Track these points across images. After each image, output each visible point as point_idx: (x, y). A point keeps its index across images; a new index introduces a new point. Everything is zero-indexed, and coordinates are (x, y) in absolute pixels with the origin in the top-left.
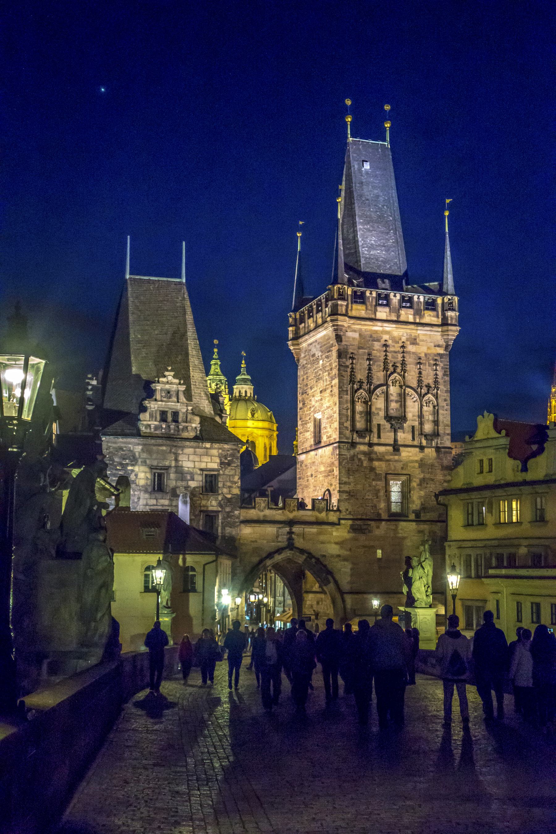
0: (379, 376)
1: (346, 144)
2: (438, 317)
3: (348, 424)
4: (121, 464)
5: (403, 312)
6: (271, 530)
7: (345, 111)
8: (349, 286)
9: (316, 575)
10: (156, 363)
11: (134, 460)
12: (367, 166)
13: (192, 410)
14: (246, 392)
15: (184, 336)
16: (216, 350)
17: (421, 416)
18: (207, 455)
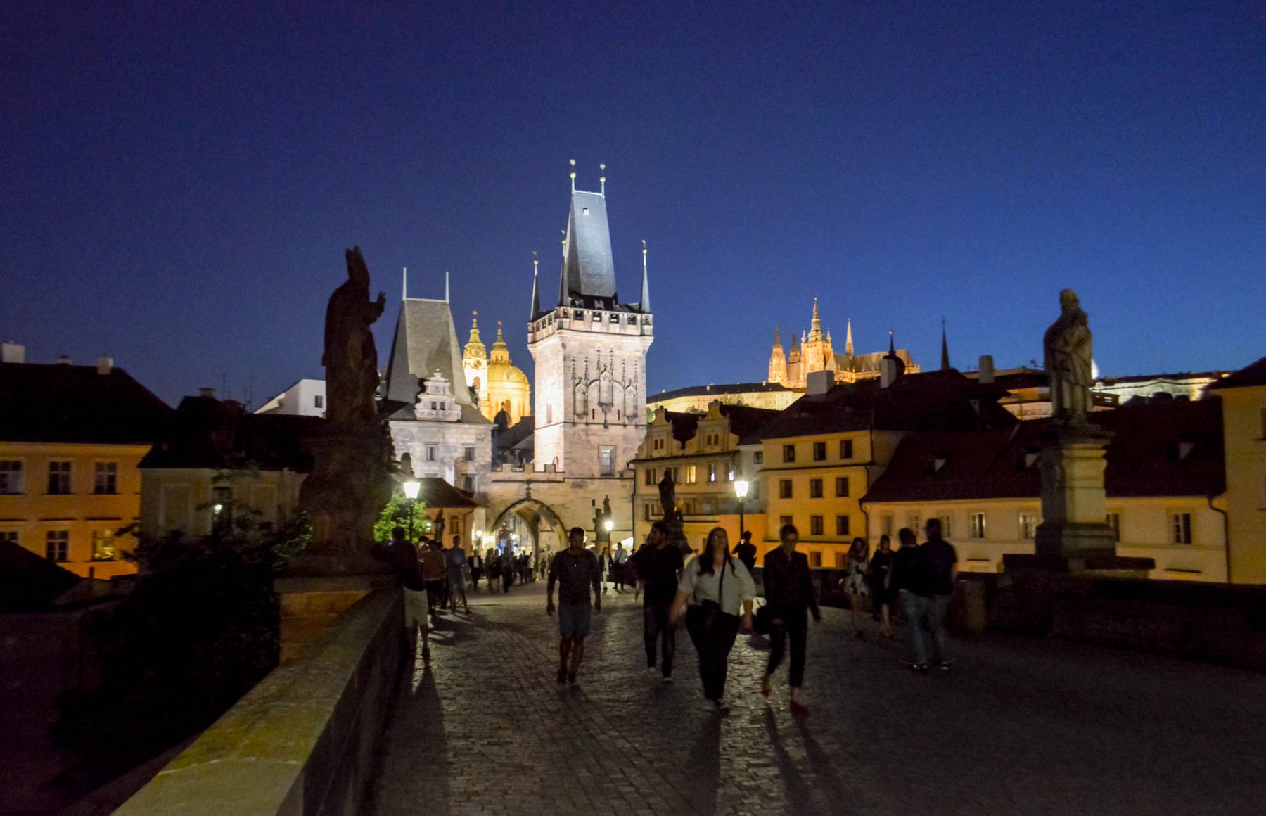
0: (593, 374)
1: (570, 194)
2: (637, 329)
3: (571, 409)
4: (403, 441)
5: (612, 326)
6: (513, 487)
7: (570, 169)
8: (571, 307)
9: (548, 518)
10: (427, 365)
11: (412, 438)
12: (587, 212)
13: (455, 401)
14: (502, 357)
15: (448, 343)
16: (475, 320)
17: (624, 402)
18: (466, 433)
